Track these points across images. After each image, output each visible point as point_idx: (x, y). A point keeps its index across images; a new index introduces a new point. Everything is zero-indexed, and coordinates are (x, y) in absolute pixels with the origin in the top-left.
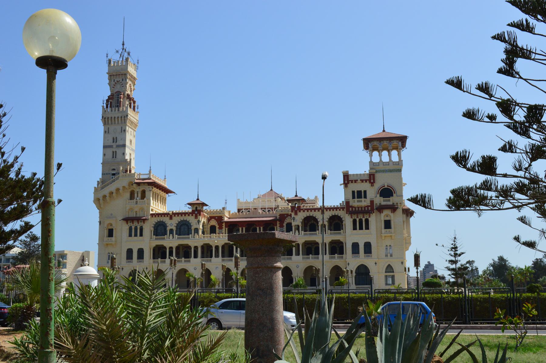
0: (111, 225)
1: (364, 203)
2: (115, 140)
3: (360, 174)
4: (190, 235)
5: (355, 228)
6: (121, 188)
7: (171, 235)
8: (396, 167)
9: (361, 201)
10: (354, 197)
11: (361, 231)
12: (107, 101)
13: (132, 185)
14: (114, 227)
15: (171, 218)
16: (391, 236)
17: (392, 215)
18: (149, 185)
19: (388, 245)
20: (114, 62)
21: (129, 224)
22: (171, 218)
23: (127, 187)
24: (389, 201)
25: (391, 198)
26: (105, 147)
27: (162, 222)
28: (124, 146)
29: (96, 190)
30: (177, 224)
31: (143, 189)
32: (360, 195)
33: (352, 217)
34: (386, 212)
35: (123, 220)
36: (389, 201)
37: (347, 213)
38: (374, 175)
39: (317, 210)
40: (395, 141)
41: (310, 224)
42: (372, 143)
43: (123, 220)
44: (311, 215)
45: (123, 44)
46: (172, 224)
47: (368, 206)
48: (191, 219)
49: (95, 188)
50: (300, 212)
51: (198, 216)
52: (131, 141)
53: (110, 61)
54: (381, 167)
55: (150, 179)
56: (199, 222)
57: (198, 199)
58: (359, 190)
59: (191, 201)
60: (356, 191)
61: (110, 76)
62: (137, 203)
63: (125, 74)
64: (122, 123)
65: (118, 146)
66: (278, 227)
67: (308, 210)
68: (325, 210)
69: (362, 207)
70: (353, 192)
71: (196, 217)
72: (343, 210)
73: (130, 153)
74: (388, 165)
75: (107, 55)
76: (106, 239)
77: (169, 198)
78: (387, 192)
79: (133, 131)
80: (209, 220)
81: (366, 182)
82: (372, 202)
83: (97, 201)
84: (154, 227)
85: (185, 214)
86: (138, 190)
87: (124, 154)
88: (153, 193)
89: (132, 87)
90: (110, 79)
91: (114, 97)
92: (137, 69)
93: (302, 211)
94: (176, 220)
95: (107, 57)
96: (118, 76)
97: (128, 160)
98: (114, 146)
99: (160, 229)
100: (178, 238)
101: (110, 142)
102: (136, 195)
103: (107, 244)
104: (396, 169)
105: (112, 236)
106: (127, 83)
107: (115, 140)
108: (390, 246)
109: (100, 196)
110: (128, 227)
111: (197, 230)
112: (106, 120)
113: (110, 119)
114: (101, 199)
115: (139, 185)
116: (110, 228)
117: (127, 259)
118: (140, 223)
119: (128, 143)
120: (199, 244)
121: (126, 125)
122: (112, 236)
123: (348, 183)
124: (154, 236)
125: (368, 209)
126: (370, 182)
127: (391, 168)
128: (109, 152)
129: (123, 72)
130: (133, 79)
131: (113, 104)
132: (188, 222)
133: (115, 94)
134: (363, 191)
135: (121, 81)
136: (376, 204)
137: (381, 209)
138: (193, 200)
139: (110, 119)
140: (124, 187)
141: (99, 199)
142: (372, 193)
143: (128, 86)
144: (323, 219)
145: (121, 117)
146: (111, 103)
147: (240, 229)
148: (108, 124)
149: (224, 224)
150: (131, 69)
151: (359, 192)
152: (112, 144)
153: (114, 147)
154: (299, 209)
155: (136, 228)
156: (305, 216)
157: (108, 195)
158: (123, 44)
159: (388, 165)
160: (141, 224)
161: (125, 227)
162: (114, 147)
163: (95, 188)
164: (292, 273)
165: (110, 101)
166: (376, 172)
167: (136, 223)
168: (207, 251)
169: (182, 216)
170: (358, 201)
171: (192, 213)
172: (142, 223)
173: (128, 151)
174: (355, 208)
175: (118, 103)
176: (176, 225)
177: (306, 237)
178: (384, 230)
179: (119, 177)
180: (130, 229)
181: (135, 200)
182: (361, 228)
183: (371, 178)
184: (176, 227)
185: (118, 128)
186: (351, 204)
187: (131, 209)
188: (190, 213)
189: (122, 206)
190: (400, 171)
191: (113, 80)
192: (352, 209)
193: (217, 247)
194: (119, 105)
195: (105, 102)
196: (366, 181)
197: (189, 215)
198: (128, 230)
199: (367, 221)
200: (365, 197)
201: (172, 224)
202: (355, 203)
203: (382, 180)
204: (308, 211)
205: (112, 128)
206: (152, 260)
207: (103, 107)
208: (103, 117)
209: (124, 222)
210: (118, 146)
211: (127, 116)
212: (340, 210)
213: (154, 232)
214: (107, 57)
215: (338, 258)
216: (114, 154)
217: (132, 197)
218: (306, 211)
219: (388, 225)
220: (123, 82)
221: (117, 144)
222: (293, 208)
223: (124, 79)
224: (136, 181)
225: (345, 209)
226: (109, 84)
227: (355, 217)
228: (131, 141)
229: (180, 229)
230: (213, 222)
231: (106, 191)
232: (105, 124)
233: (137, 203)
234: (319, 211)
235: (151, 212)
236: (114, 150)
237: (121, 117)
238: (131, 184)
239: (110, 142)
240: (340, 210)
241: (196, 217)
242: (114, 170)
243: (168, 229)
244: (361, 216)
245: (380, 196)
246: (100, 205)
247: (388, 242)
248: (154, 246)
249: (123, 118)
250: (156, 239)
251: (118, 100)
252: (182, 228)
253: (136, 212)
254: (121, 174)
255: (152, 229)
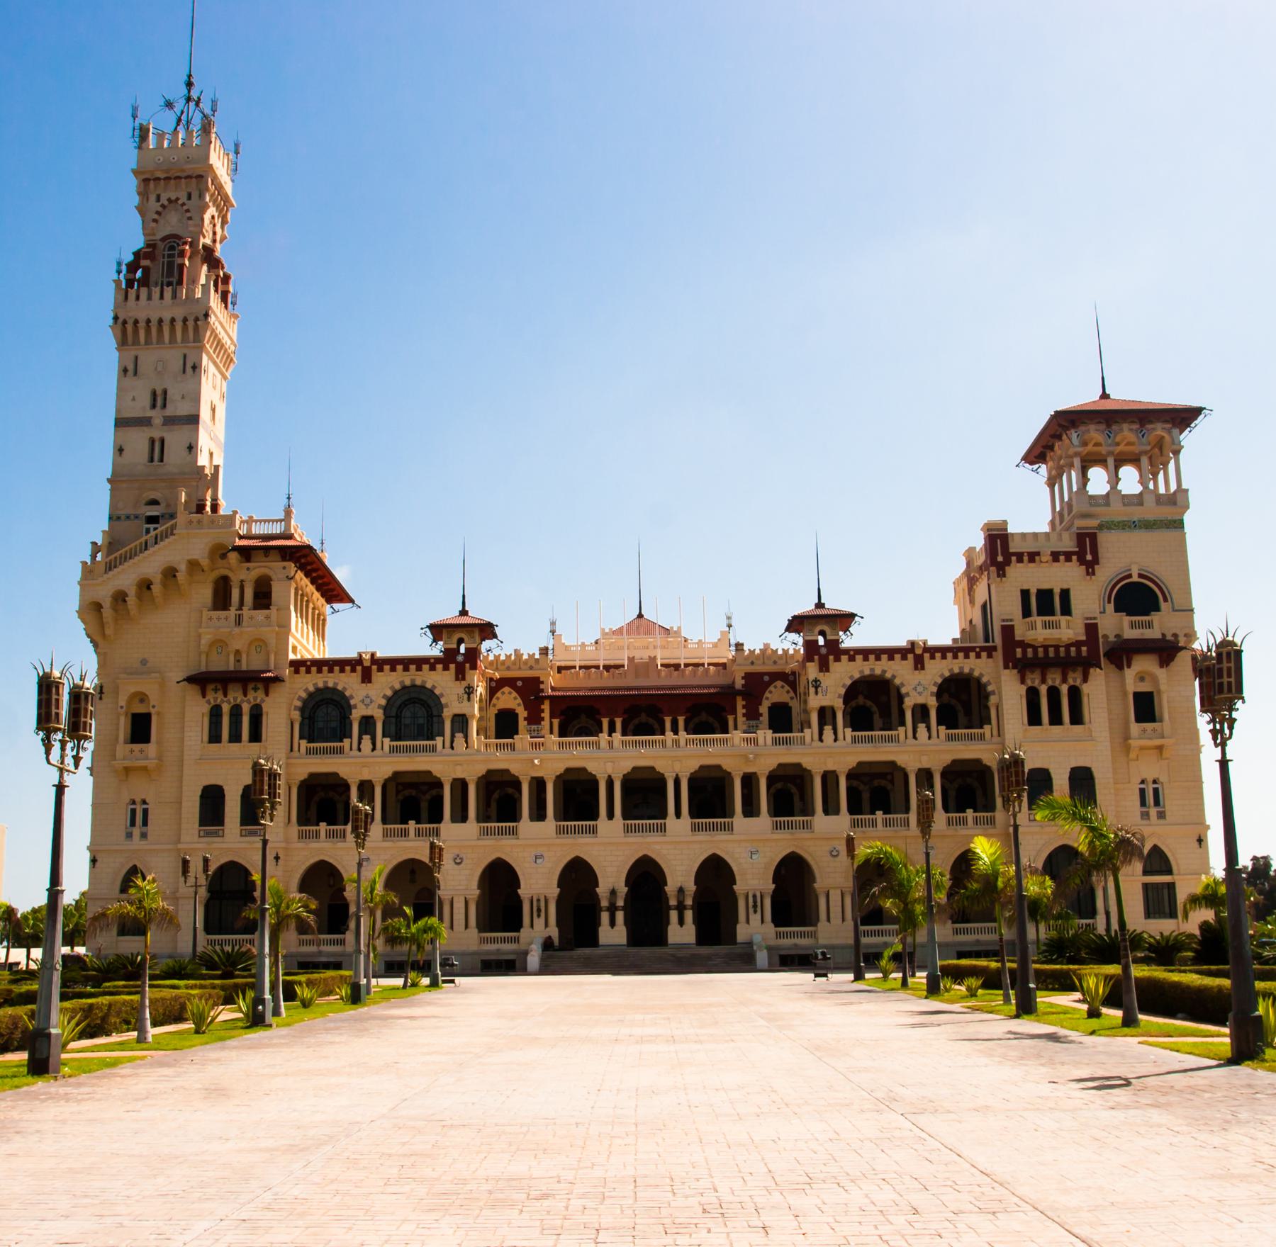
0: (143, 698)
1: (1068, 630)
2: (159, 399)
3: (1035, 535)
4: (439, 740)
5: (1034, 719)
6: (183, 567)
7: (366, 738)
8: (1166, 512)
9: (1056, 626)
10: (1026, 613)
11: (1056, 728)
12: (132, 267)
13: (224, 556)
14: (155, 706)
15: (367, 677)
16: (1160, 748)
17: (1161, 674)
18: (284, 559)
19: (1150, 779)
20: (160, 136)
21: (211, 695)
22: (367, 677)
23: (205, 562)
24: (1149, 625)
25: (1155, 617)
26: (121, 423)
27: (334, 690)
28: (194, 420)
29: (88, 572)
30: (389, 700)
31: (266, 571)
32: (1046, 603)
33: (1023, 682)
34: (1145, 664)
35: (190, 680)
36: (1149, 625)
37: (1006, 667)
38: (1093, 537)
39: (897, 657)
40: (1159, 426)
41: (873, 703)
42: (1082, 428)
43: (190, 680)
44: (878, 672)
45: (189, 84)
46: (368, 699)
47: (1078, 644)
48: (442, 682)
49: (84, 563)
50: (837, 659)
51: (469, 673)
52: (213, 410)
53: (143, 133)
54: (1116, 512)
55: (291, 537)
56: (470, 691)
57: (464, 613)
58: (1046, 586)
59: (435, 620)
60: (1033, 591)
61: (146, 181)
62: (239, 621)
63: (200, 177)
64: (185, 339)
65: (170, 421)
66: (741, 719)
67: (866, 653)
68: (927, 656)
69: (1057, 647)
70: (1025, 594)
71: (460, 675)
72: (990, 656)
73: (211, 445)
74: (1141, 504)
75: (135, 109)
76: (123, 749)
77: (338, 617)
78: (1138, 597)
79: (219, 376)
80: (495, 687)
81: (1068, 559)
82: (1091, 629)
83: (92, 612)
84: (302, 710)
85: (419, 662)
86: (244, 575)
87: (192, 448)
88: (296, 589)
89: (218, 229)
90: (143, 194)
91: (158, 252)
92: (234, 170)
93: (844, 658)
94: (386, 683)
95: (134, 117)
96: (174, 185)
97: (207, 471)
98: (158, 421)
99: (325, 717)
100: (393, 750)
101: (142, 407)
102: (235, 593)
103: (127, 770)
104: (1167, 516)
105: (146, 739)
106: (206, 207)
107: (159, 399)
108: (1155, 782)
109: (104, 594)
110: (206, 709)
111: (461, 722)
112: (129, 327)
113: (142, 325)
114: (107, 604)
115: (248, 560)
116: (140, 709)
117: (203, 822)
118: (251, 695)
119: (205, 414)
120: (472, 772)
121: (201, 348)
122: (146, 739)
123: (1007, 562)
124: (304, 743)
125: (1079, 651)
126: (1082, 561)
127: (1151, 517)
128: (138, 440)
129: (190, 168)
130: (224, 203)
131: (154, 276)
132: (431, 691)
133: (161, 245)
134: (1057, 591)
135: (183, 199)
136: (1105, 636)
137: (1121, 654)
138: (448, 613)
139: (142, 325)
140: (193, 565)
141: (98, 607)
142: (1089, 598)
143: (207, 217)
144: (919, 687)
145: (185, 320)
146: (146, 271)
147: (605, 722)
148: (136, 342)
149: (546, 706)
150: (218, 161)
151: (1045, 596)
152: (149, 413)
153: (155, 426)
154: (834, 649)
155: (236, 712)
156: (857, 676)
157: (132, 592)
158: (189, 84)
159: (1141, 504)
160: (255, 696)
161: (197, 709)
162: (155, 426)
163: (84, 563)
164: (813, 879)
165: (145, 263)
166: (1101, 527)
167: (235, 695)
168: (500, 799)
169: (406, 669)
170: (1046, 625)
171: (449, 657)
172: (260, 695)
173: (205, 441)
174: (1035, 648)
175: (170, 274)
176: (383, 702)
177: (861, 747)
178: (1135, 728)
179: (173, 527)
180: (215, 713)
181: (233, 612)
182: (1056, 719)
183: (1085, 550)
184: (386, 709)
185: (173, 357)
186: (1019, 635)
187: (219, 644)
188: (438, 660)
189: (181, 632)
190: (1178, 525)
191: (153, 198)
192: (1024, 653)
193: (538, 784)
194: (174, 277)
195: (124, 268)
196: (1068, 556)
197: (433, 668)
198: (206, 720)
199: (1075, 694)
200: (1066, 610)
201: (368, 699)
202: (1037, 632)
203: (1124, 555)
204: (866, 659)
205: (148, 358)
206: (295, 829)
207: (118, 282)
208: (116, 318)
209: (192, 692)
210: (170, 421)
211: (207, 315)
212: (978, 656)
213: (301, 725)
214: (134, 117)
215: (976, 821)
216: (157, 449)
217: (221, 598)
218: (859, 658)
219: (1146, 707)
220: (189, 204)
221: (169, 411)
222: (810, 646)
223: (195, 195)
224: (238, 542)
225: (999, 655)
226: (141, 210)
227: (1034, 679)
228: (213, 410)
229: (398, 717)
230: (509, 699)
231: (126, 578)
232: (123, 342)
233: (239, 621)
234: (904, 658)
235: (291, 656)
236: (156, 434)
237: (185, 320)
238: (220, 552)
239: (142, 407)
240: (978, 656)
241: (460, 675)
242: (154, 502)
243: (356, 715)
244: (1054, 678)
245: (1116, 611)
246: (102, 625)
247: (1149, 769)
248: (303, 776)
249: (190, 324)
250: (310, 752)
251: (171, 264)
252: (407, 713)
253: (238, 652)
254: (182, 518)
255: (296, 715)
